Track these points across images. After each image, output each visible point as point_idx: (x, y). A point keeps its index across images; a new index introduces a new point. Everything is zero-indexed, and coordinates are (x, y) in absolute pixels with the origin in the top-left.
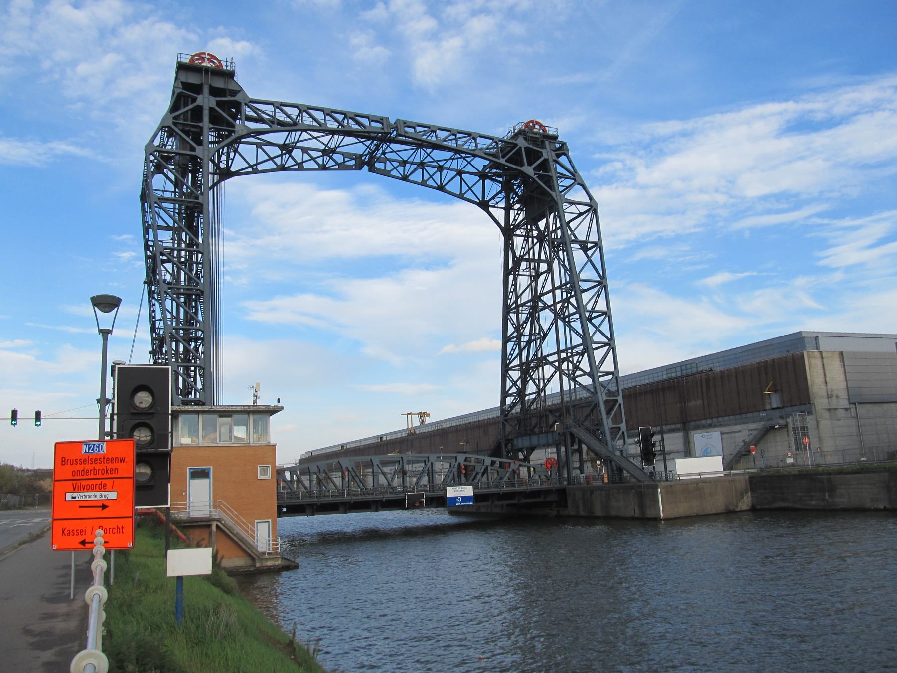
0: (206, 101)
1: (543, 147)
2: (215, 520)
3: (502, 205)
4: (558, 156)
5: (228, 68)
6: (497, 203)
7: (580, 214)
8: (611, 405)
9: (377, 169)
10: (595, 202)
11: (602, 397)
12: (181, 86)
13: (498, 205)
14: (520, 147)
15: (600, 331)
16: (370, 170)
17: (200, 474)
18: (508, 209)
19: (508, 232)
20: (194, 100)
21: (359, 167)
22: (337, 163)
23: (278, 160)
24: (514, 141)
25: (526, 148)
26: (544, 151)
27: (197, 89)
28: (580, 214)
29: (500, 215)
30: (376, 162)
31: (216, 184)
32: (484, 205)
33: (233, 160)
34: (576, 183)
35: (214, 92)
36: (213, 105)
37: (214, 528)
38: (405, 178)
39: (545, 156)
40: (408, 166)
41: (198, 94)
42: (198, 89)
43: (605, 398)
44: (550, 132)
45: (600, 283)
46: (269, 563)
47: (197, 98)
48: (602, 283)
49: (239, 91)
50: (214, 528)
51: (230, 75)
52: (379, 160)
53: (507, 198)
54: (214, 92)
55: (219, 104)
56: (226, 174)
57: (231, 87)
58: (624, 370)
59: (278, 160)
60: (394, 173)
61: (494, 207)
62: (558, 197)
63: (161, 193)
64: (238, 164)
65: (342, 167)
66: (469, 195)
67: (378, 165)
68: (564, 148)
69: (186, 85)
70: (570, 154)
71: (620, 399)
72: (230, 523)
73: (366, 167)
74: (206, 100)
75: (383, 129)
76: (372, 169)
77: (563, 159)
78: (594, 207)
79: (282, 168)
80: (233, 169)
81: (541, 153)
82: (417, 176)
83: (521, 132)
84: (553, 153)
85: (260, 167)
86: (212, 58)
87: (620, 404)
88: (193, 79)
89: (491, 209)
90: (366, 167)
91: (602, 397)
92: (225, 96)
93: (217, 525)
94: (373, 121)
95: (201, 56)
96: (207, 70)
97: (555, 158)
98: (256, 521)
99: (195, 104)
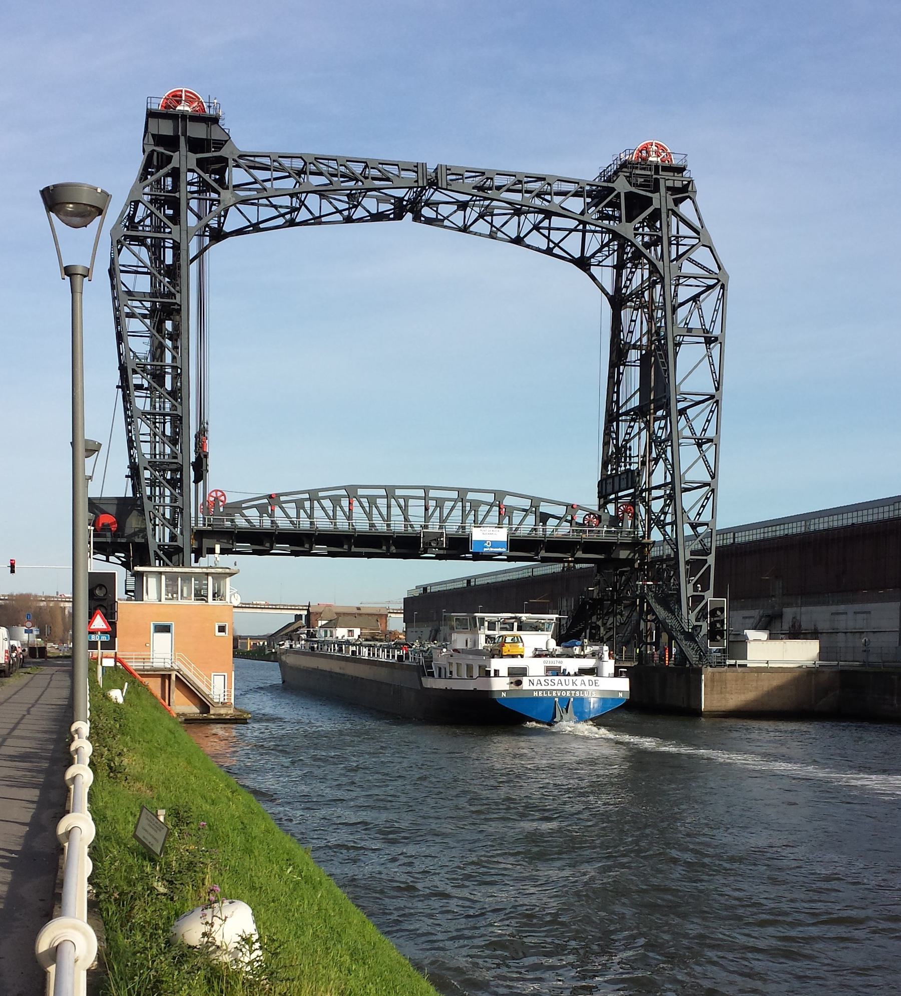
0: (184, 159)
1: (656, 189)
2: (174, 670)
3: (612, 260)
4: (677, 202)
5: (212, 113)
6: (600, 262)
7: (709, 288)
8: (694, 566)
9: (424, 217)
10: (726, 274)
11: (685, 555)
12: (151, 141)
13: (603, 263)
14: (619, 194)
15: (706, 461)
16: (415, 219)
17: (165, 629)
18: (619, 267)
19: (617, 301)
20: (169, 159)
21: (399, 216)
22: (371, 215)
23: (288, 217)
24: (610, 185)
25: (628, 195)
26: (655, 197)
27: (171, 142)
28: (709, 288)
29: (606, 276)
30: (422, 207)
31: (202, 251)
32: (583, 263)
33: (223, 223)
34: (700, 244)
35: (196, 145)
36: (193, 164)
37: (173, 678)
38: (465, 229)
39: (656, 204)
40: (469, 210)
41: (174, 152)
42: (171, 142)
43: (688, 557)
44: (676, 161)
45: (712, 397)
46: (223, 711)
47: (172, 156)
48: (714, 399)
49: (226, 141)
50: (173, 678)
51: (215, 120)
52: (428, 204)
53: (621, 250)
54: (196, 145)
55: (201, 163)
56: (218, 235)
57: (216, 135)
58: (721, 525)
59: (288, 217)
60: (446, 223)
61: (598, 265)
62: (667, 269)
63: (135, 268)
64: (233, 222)
65: (378, 217)
66: (557, 251)
67: (427, 212)
68: (690, 189)
69: (159, 140)
70: (698, 199)
71: (711, 559)
72: (190, 675)
73: (409, 216)
74: (183, 158)
75: (417, 181)
76: (417, 217)
77: (686, 208)
78: (722, 281)
79: (292, 223)
80: (227, 228)
81: (651, 198)
82: (482, 227)
83: (624, 165)
84: (670, 199)
85: (262, 226)
86: (191, 99)
87: (710, 566)
88: (166, 128)
89: (593, 270)
90: (409, 216)
91: (685, 555)
92: (209, 151)
93: (176, 676)
94: (403, 170)
95: (176, 98)
96: (184, 116)
97: (671, 205)
98: (213, 674)
99: (170, 167)
